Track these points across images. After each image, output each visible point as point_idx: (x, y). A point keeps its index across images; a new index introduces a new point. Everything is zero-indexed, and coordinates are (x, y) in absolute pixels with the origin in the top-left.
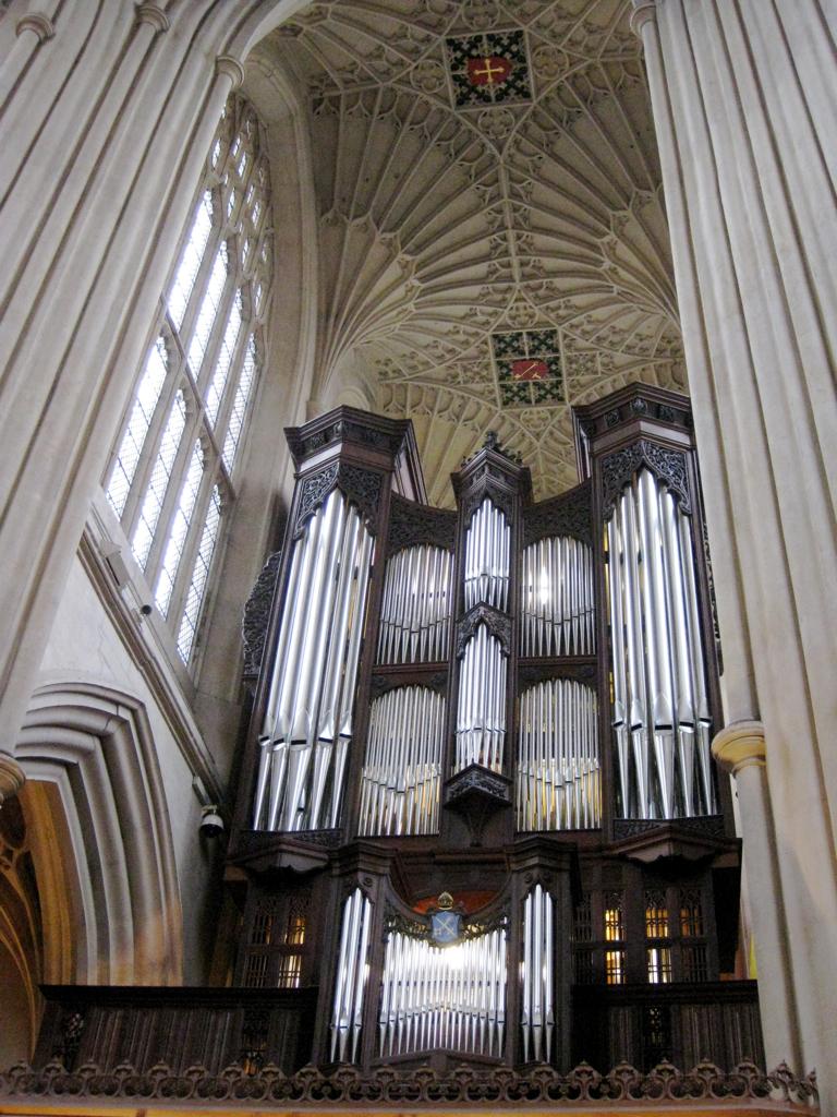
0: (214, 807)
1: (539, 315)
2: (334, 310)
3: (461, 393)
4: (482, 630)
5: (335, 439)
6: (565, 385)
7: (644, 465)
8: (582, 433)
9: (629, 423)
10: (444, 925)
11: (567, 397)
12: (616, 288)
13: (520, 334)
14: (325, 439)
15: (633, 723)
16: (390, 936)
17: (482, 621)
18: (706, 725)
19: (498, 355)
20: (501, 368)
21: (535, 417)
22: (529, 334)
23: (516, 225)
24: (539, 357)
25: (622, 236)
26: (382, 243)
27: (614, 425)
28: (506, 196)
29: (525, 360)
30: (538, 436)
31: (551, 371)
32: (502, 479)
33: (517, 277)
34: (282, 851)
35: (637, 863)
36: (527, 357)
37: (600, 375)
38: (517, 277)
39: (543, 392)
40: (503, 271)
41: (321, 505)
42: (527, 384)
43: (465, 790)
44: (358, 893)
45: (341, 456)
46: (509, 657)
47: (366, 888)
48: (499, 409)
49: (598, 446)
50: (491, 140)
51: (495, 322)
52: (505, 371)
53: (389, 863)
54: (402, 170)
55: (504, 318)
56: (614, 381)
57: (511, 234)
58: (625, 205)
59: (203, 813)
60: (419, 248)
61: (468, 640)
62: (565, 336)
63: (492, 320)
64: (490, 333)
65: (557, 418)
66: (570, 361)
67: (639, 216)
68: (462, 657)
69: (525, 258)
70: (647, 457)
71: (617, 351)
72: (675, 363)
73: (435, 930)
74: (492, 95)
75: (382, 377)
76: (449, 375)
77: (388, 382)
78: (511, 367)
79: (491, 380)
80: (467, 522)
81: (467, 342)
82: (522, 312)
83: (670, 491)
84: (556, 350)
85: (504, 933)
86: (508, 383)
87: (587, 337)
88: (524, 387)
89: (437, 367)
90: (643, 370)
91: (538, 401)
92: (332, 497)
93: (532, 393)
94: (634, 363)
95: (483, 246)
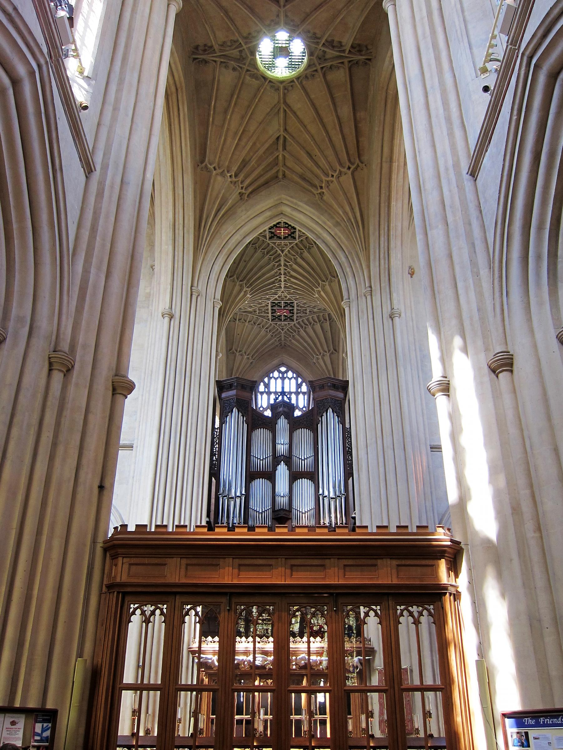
14: (230, 387)
19: (272, 307)
25: (323, 290)
28: (282, 265)
31: (290, 312)
38: (283, 287)
43: (279, 516)
50: (280, 250)
52: (274, 311)
54: (247, 259)
60: (251, 285)
62: (297, 303)
66: (298, 310)
67: (330, 285)
74: (282, 237)
84: (293, 307)
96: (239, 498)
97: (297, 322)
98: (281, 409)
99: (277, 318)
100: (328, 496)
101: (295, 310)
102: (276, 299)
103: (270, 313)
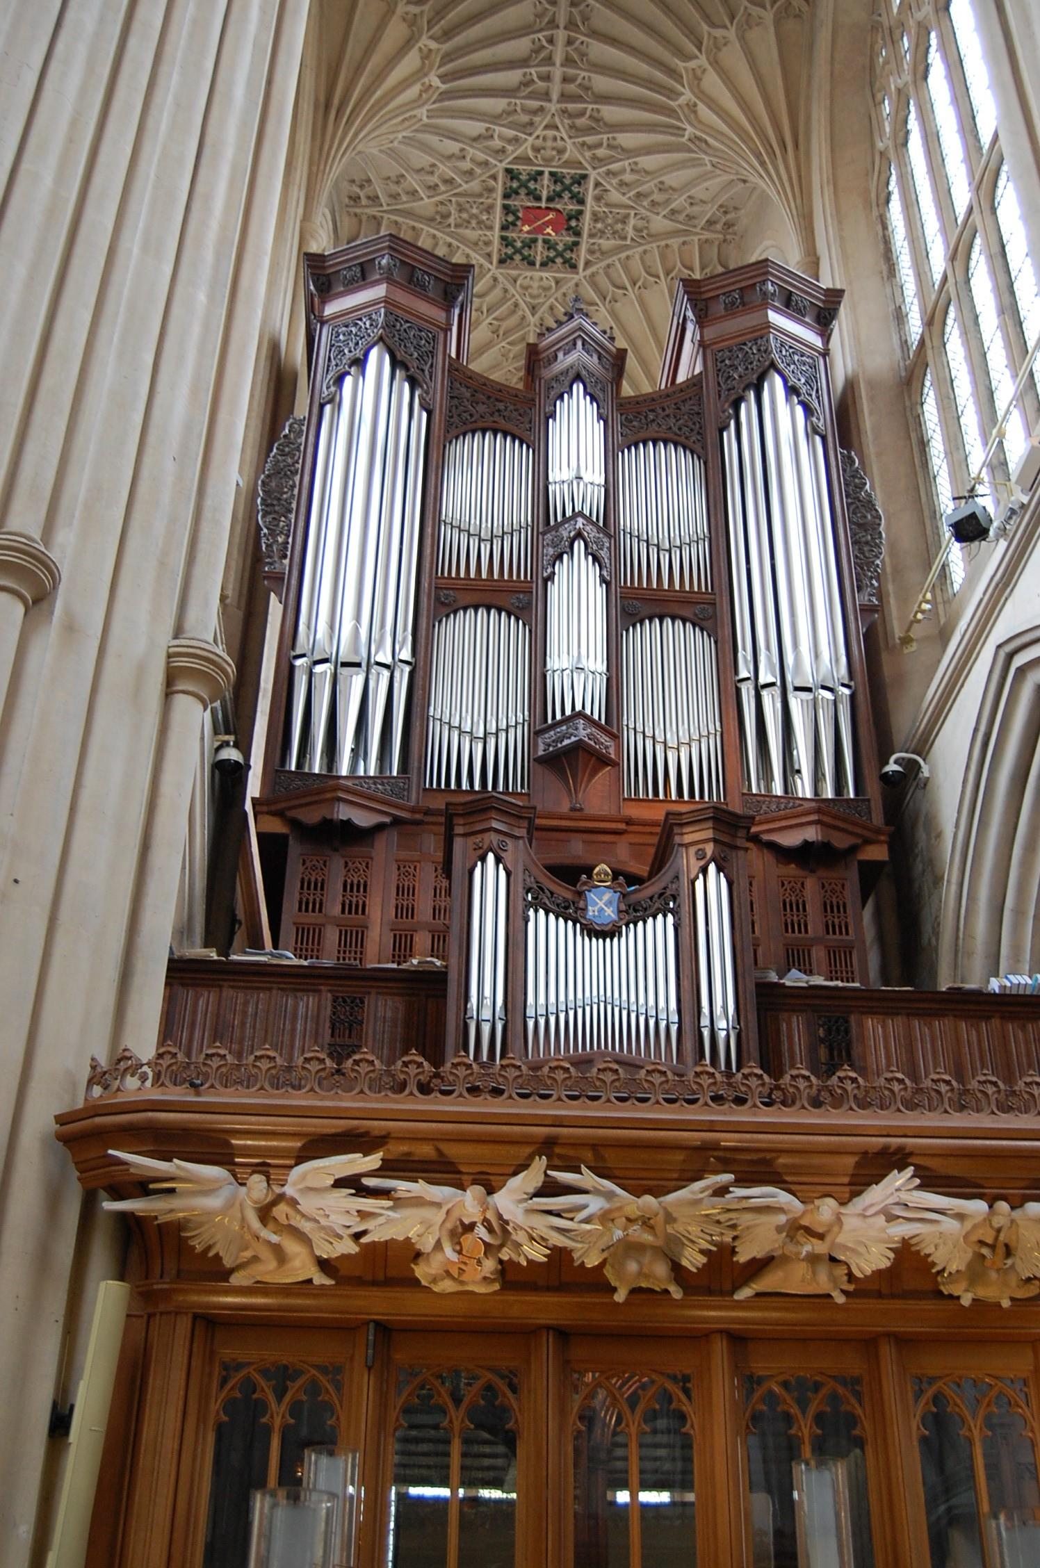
0: (231, 738)
1: (571, 152)
2: (336, 101)
3: (449, 240)
4: (579, 546)
5: (378, 277)
6: (583, 248)
7: (773, 365)
8: (690, 314)
9: (755, 308)
10: (601, 904)
11: (581, 265)
12: (690, 130)
13: (541, 173)
14: (362, 275)
15: (762, 681)
16: (531, 913)
17: (579, 535)
18: (847, 691)
19: (506, 196)
20: (507, 214)
21: (535, 285)
22: (552, 174)
23: (571, 25)
24: (559, 206)
25: (715, 63)
26: (404, 20)
27: (732, 309)
29: (540, 208)
30: (534, 309)
31: (569, 228)
32: (595, 357)
33: (555, 96)
34: (340, 799)
35: (773, 847)
36: (543, 205)
37: (628, 242)
38: (555, 96)
39: (552, 254)
40: (541, 85)
41: (360, 363)
42: (535, 241)
43: (566, 742)
44: (491, 857)
45: (387, 301)
46: (608, 584)
47: (503, 854)
48: (493, 267)
49: (710, 333)
51: (513, 152)
52: (511, 218)
53: (525, 824)
55: (526, 148)
56: (645, 252)
57: (561, 35)
58: (728, 24)
59: (217, 744)
60: (447, 35)
61: (559, 557)
62: (597, 184)
63: (510, 148)
64: (504, 165)
65: (563, 290)
66: (596, 218)
68: (551, 577)
69: (571, 71)
70: (776, 356)
71: (658, 214)
72: (725, 241)
73: (590, 908)
75: (352, 203)
76: (437, 212)
77: (358, 210)
78: (520, 215)
79: (491, 228)
80: (549, 409)
81: (470, 173)
82: (549, 144)
83: (802, 403)
84: (581, 202)
85: (670, 918)
86: (511, 235)
87: (625, 189)
88: (531, 243)
89: (426, 200)
90: (684, 243)
91: (543, 264)
92: (374, 354)
93: (540, 253)
94: (675, 233)
95: (522, 46)
96: (386, 674)
97: (589, 272)
98: (572, 358)
99: (517, 251)
100: (778, 683)
101: (586, 222)
102: (526, 160)
103: (497, 227)
